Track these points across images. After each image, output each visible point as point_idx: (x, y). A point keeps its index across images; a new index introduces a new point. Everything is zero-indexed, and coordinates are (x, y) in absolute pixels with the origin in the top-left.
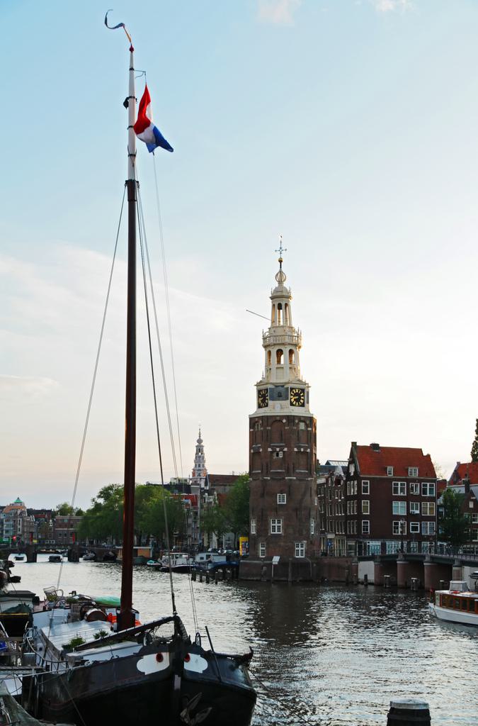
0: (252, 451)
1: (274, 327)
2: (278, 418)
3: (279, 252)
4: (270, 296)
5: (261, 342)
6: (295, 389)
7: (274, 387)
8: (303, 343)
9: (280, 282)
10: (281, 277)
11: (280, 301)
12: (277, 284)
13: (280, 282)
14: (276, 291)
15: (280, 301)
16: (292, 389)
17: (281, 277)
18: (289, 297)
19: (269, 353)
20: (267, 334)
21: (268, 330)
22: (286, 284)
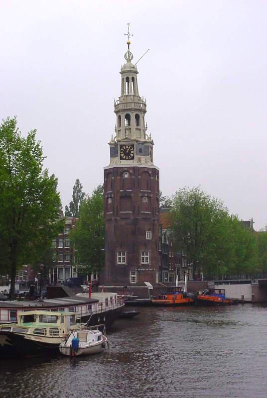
3: (127, 36)
6: (125, 146)
7: (114, 146)
9: (129, 60)
10: (129, 57)
11: (129, 76)
13: (129, 60)
14: (124, 67)
15: (129, 76)
16: (121, 146)
17: (129, 57)
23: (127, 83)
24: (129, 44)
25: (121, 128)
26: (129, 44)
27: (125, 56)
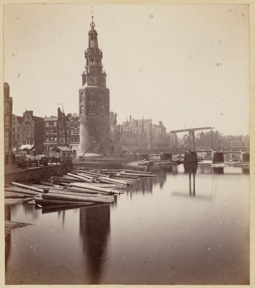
0: (80, 105)
1: (90, 49)
2: (92, 90)
4: (88, 33)
5: (84, 55)
8: (103, 56)
9: (93, 27)
10: (93, 25)
11: (93, 35)
12: (91, 28)
13: (93, 27)
14: (91, 31)
15: (93, 35)
17: (93, 25)
18: (97, 35)
19: (88, 61)
20: (87, 51)
21: (87, 50)
22: (95, 28)
23: (91, 41)
24: (93, 17)
25: (88, 67)
26: (93, 17)
27: (91, 25)
